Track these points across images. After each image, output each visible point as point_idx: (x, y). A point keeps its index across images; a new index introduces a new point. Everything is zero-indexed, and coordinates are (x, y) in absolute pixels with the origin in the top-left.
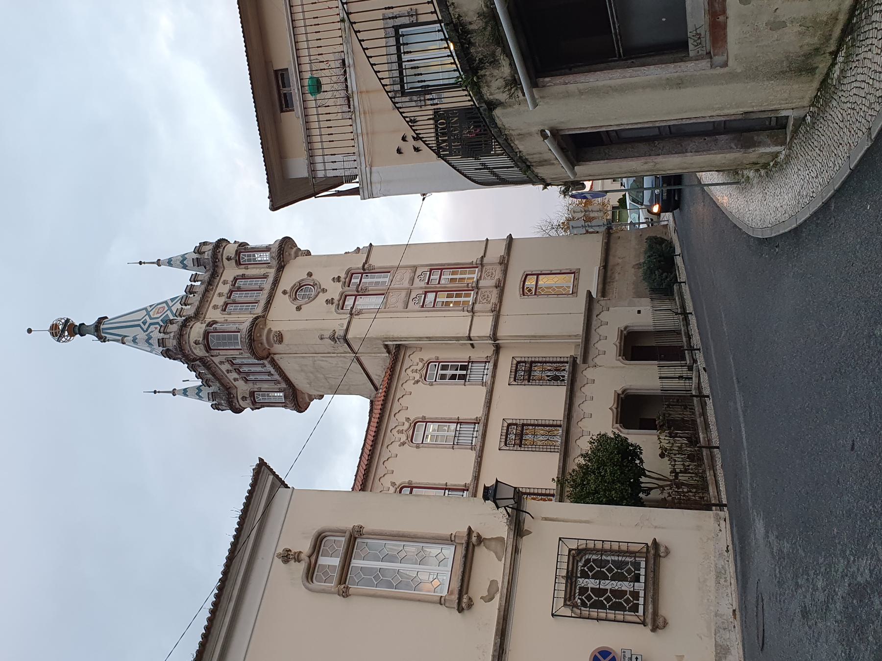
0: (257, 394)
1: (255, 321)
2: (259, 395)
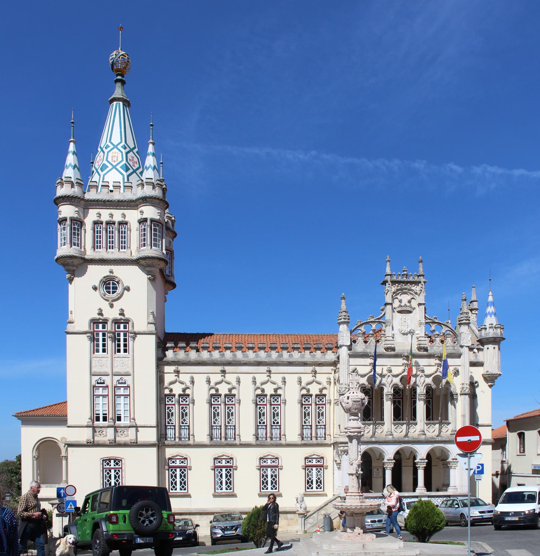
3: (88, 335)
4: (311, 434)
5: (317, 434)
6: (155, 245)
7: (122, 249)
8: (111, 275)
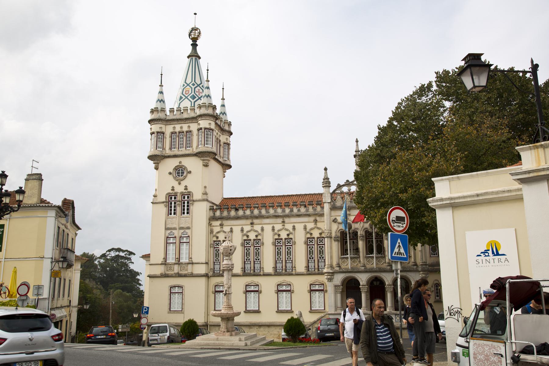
2: (162, 136)
3: (165, 204)
4: (315, 267)
5: (319, 266)
7: (188, 148)
8: (180, 164)
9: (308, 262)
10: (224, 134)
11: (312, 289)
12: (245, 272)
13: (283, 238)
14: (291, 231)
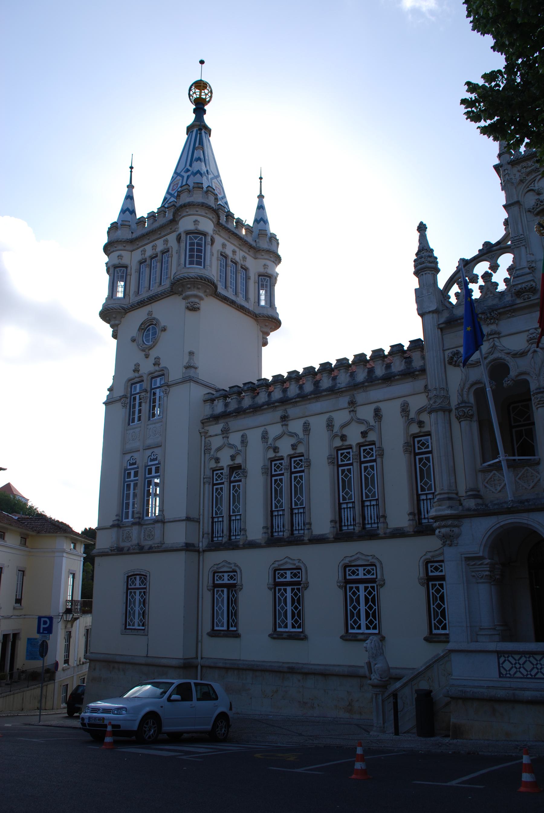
0: (124, 270)
1: (211, 283)
6: (191, 263)
9: (419, 500)
10: (260, 256)
11: (431, 574)
12: (272, 536)
13: (354, 444)
14: (372, 422)
